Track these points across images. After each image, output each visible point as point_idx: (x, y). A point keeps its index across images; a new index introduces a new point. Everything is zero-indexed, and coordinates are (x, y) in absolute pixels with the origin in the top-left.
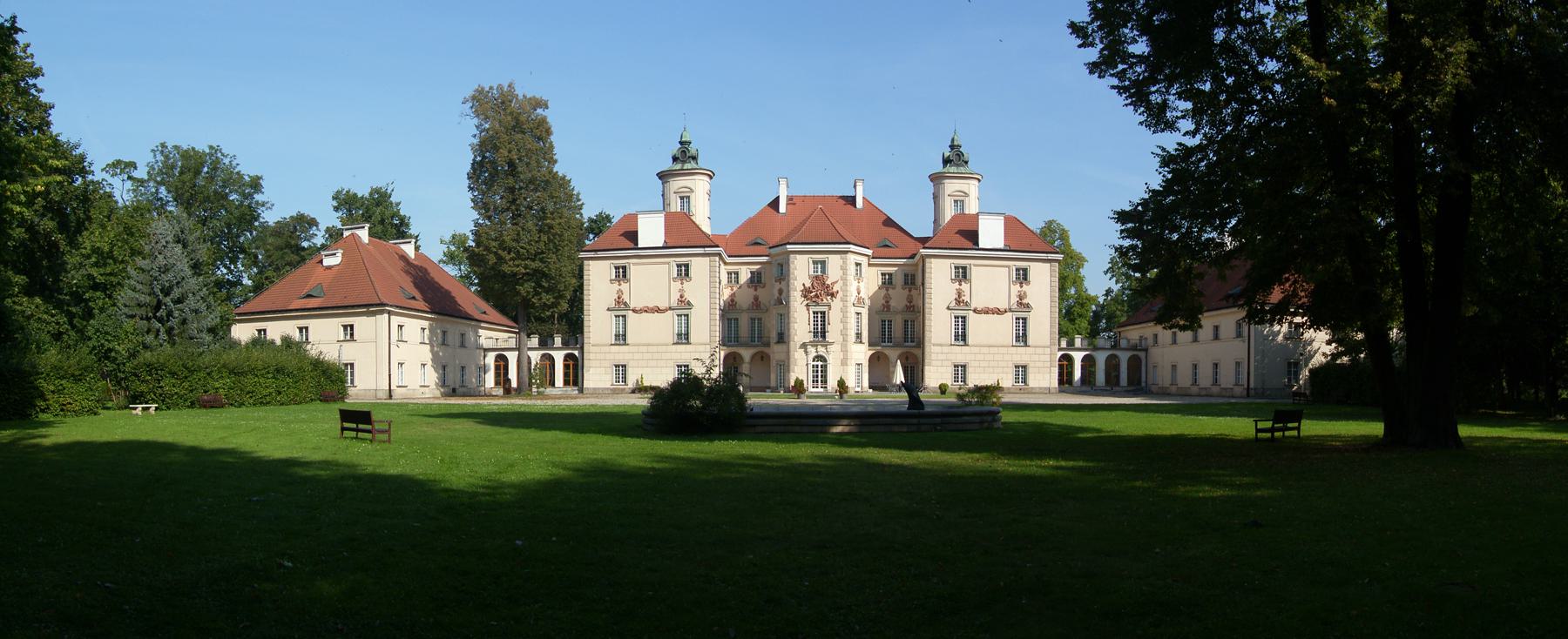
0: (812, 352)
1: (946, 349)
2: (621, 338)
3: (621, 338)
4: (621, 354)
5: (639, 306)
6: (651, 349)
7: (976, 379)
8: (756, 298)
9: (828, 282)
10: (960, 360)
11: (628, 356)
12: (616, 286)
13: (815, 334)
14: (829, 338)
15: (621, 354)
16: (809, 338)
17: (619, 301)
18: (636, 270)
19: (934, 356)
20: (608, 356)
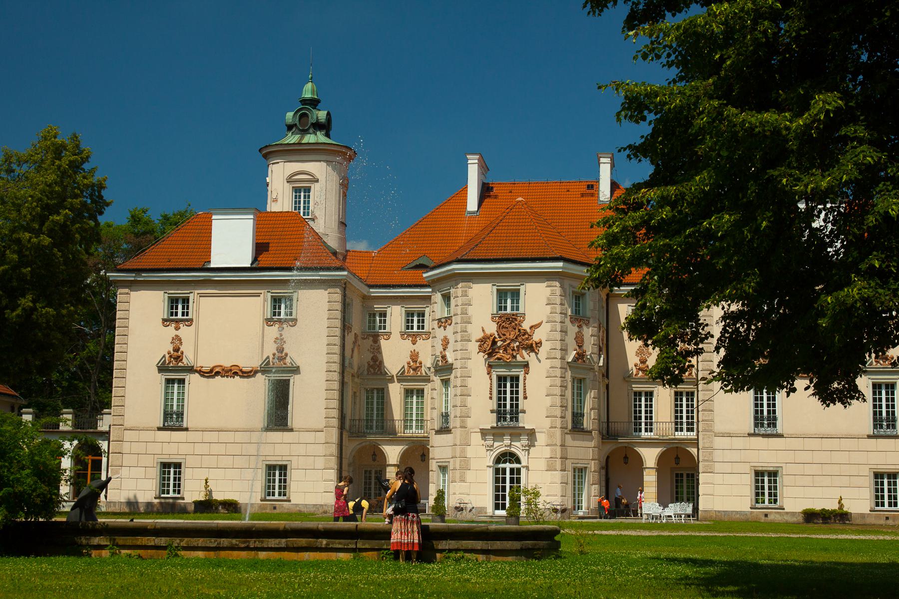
0: (500, 447)
1: (738, 443)
2: (173, 420)
3: (173, 420)
4: (172, 445)
5: (206, 363)
6: (224, 436)
7: (795, 499)
8: (414, 356)
9: (526, 326)
10: (767, 461)
11: (184, 449)
12: (171, 331)
13: (500, 414)
14: (526, 421)
15: (172, 445)
16: (490, 421)
17: (177, 354)
18: (208, 308)
19: (718, 455)
20: (152, 448)
